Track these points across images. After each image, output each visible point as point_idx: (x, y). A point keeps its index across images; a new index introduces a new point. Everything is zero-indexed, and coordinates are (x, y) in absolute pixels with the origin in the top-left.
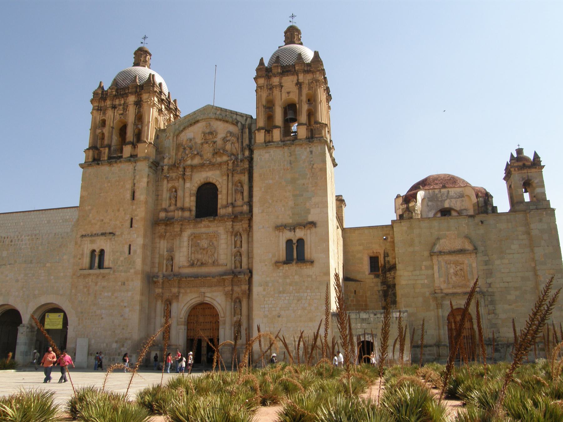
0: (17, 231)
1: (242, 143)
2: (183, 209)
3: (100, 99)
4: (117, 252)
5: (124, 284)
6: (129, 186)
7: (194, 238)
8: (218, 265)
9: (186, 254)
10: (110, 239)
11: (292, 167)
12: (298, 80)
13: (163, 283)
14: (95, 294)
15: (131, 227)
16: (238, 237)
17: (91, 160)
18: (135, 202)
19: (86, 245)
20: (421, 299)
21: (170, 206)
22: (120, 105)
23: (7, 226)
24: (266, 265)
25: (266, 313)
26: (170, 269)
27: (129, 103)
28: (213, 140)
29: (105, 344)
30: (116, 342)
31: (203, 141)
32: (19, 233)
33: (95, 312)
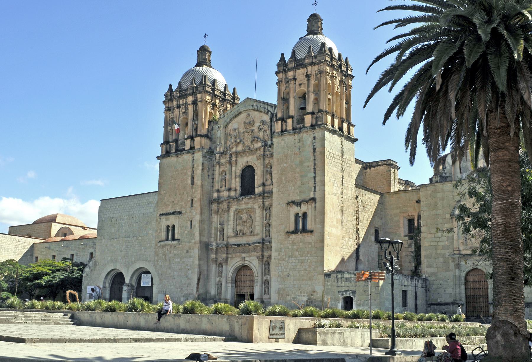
1: (271, 130)
2: (229, 190)
3: (168, 101)
4: (183, 227)
5: (187, 252)
6: (190, 173)
7: (238, 212)
8: (254, 235)
9: (232, 226)
11: (300, 152)
12: (307, 73)
13: (217, 250)
14: (170, 260)
15: (192, 207)
16: (268, 211)
17: (164, 153)
18: (194, 186)
20: (441, 260)
21: (221, 187)
22: (183, 105)
24: (281, 235)
25: (280, 273)
26: (222, 239)
27: (189, 103)
28: (251, 129)
29: (176, 299)
30: (183, 296)
31: (245, 130)
32: (121, 214)
33: (170, 274)
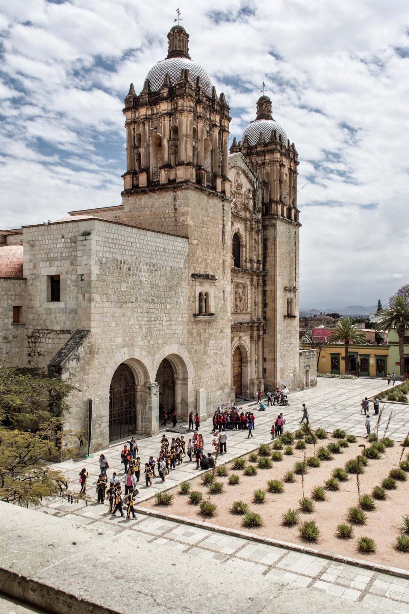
0: (134, 255)
5: (222, 332)
6: (221, 226)
8: (248, 313)
10: (213, 283)
14: (205, 342)
18: (225, 246)
19: (197, 286)
22: (208, 119)
23: (122, 245)
30: (219, 389)
32: (137, 258)
33: (206, 361)
